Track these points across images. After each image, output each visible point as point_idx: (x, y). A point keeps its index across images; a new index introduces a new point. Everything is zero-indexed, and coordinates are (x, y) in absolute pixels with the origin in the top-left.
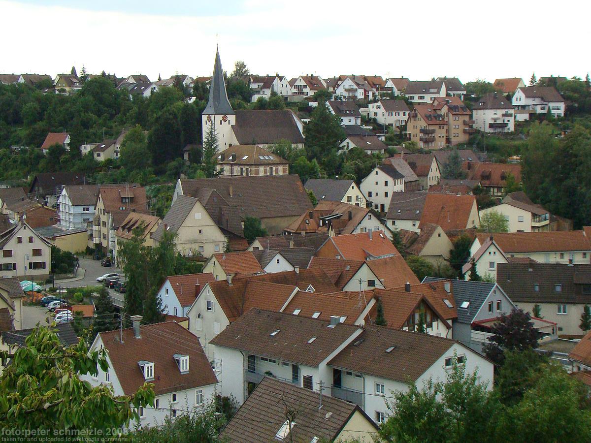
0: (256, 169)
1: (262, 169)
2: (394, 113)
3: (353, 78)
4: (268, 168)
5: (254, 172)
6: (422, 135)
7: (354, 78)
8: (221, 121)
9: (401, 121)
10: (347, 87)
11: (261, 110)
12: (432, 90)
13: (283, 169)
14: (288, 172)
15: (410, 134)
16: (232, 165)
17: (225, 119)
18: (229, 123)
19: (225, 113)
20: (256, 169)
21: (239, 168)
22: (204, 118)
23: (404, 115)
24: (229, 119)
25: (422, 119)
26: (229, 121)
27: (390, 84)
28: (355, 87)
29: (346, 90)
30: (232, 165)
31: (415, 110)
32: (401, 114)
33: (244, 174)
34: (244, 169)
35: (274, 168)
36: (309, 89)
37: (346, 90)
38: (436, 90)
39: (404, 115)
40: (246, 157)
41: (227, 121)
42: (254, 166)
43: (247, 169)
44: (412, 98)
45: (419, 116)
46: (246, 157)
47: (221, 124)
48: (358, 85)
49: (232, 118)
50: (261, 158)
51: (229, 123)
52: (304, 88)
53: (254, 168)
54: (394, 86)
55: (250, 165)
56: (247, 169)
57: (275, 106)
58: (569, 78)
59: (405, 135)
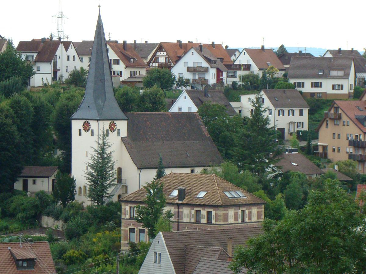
0: (225, 212)
1: (231, 212)
2: (286, 112)
3: (200, 48)
4: (240, 212)
5: (221, 218)
6: (351, 150)
7: (201, 50)
8: (80, 131)
9: (296, 124)
10: (191, 65)
11: (153, 113)
12: (334, 73)
13: (258, 212)
14: (263, 217)
15: (325, 148)
16: (178, 205)
17: (112, 128)
18: (119, 134)
19: (113, 120)
20: (225, 212)
21: (193, 212)
22: (76, 125)
23: (301, 114)
24: (118, 127)
25: (351, 123)
26: (119, 131)
27: (244, 59)
28: (205, 64)
29: (189, 70)
30: (178, 205)
31: (337, 108)
32: (297, 112)
33: (204, 221)
34: (204, 212)
35: (247, 212)
36: (124, 66)
37: (189, 70)
38: (341, 73)
39: (301, 114)
40: (202, 194)
41: (90, 131)
42: (221, 209)
43: (209, 213)
44: (301, 85)
45: (344, 118)
46: (202, 194)
47: (80, 134)
48: (209, 61)
49: (122, 126)
50: (227, 194)
51: (119, 134)
52: (114, 63)
53: (221, 212)
54: (251, 62)
55: (215, 207)
56: (209, 213)
57: (154, 103)
58: (318, 48)
59: (316, 147)
